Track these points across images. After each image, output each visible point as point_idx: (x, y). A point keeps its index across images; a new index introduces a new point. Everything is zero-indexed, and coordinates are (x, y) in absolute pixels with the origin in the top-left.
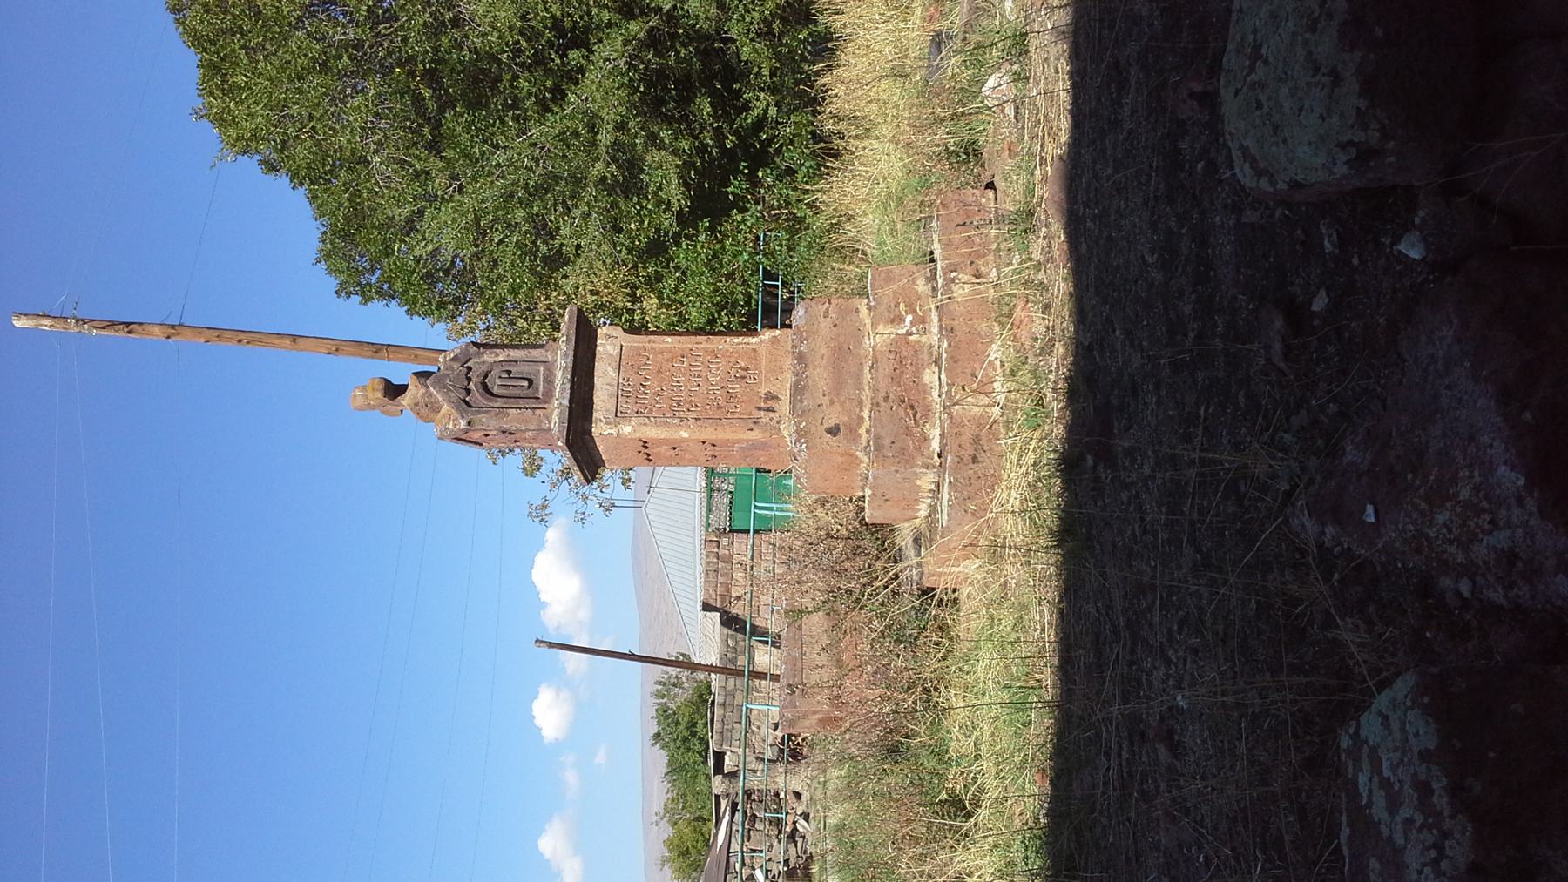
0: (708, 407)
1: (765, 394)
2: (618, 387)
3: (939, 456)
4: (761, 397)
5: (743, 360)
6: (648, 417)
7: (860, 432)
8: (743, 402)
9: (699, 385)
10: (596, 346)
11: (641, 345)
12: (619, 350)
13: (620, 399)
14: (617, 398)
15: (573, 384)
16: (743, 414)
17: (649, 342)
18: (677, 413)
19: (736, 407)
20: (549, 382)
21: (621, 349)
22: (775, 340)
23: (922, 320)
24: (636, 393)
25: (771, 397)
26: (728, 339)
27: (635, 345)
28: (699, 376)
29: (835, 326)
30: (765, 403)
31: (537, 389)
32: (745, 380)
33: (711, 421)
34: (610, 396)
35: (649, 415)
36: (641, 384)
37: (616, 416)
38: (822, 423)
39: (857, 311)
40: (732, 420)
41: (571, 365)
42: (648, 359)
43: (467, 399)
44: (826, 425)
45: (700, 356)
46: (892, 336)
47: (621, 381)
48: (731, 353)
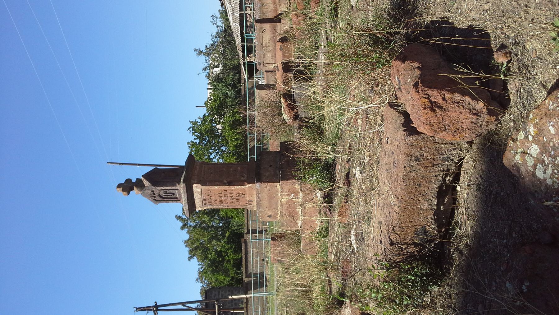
15: (188, 203)
20: (180, 194)
23: (297, 195)
25: (250, 201)
26: (235, 187)
29: (269, 190)
31: (176, 195)
34: (200, 201)
39: (276, 186)
41: (187, 199)
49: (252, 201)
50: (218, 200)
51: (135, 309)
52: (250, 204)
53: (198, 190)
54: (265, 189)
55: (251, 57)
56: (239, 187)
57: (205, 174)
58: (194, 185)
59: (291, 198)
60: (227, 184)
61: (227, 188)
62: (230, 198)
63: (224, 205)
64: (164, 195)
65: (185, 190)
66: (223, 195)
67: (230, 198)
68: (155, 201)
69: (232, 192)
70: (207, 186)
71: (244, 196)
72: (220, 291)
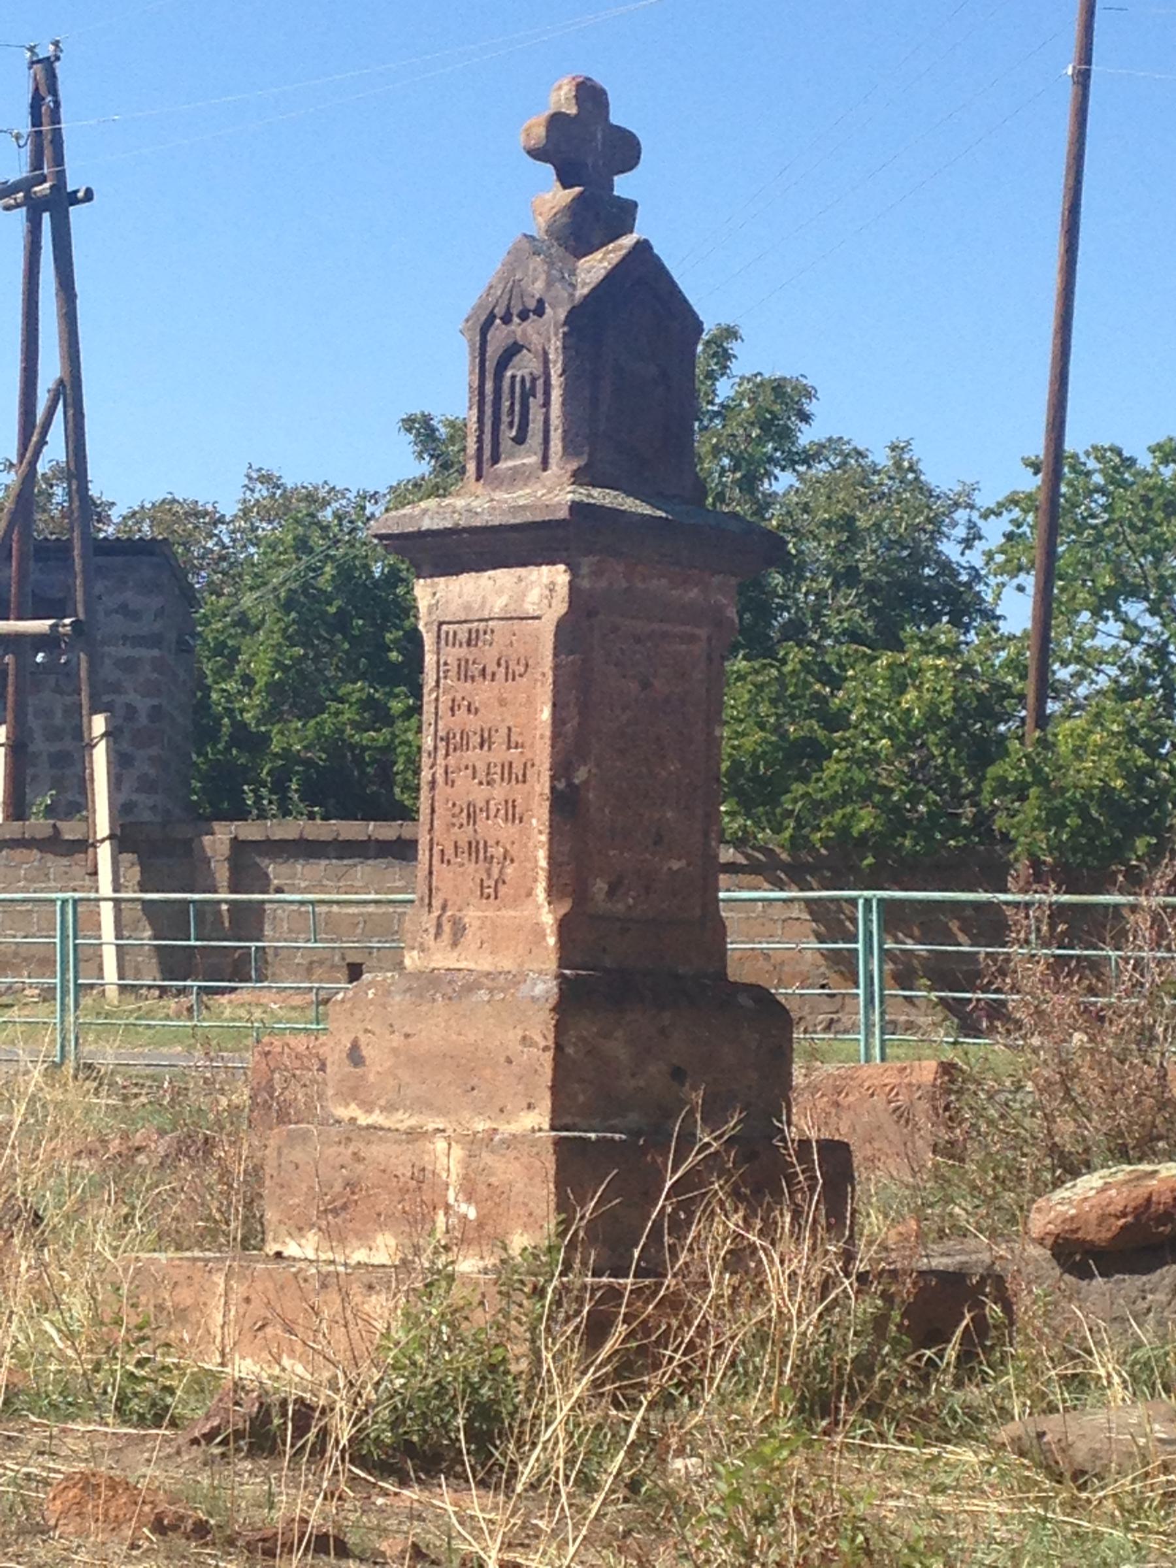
3: (279, 1255)
7: (353, 1106)
10: (539, 565)
12: (531, 613)
14: (465, 622)
20: (517, 477)
22: (538, 933)
25: (460, 930)
26: (544, 838)
31: (511, 456)
34: (467, 607)
37: (441, 624)
38: (366, 1031)
39: (530, 1107)
41: (478, 522)
43: (498, 321)
44: (363, 1039)
46: (444, 1175)
49: (455, 944)
50: (473, 723)
51: (48, 51)
52: (439, 926)
53: (534, 595)
54: (520, 1033)
56: (543, 863)
57: (638, 640)
58: (559, 575)
59: (451, 1201)
60: (561, 785)
61: (541, 784)
62: (481, 804)
63: (440, 761)
64: (513, 377)
65: (528, 517)
66: (499, 754)
67: (481, 804)
68: (483, 318)
69: (513, 813)
70: (555, 655)
71: (491, 891)
72: (156, 652)
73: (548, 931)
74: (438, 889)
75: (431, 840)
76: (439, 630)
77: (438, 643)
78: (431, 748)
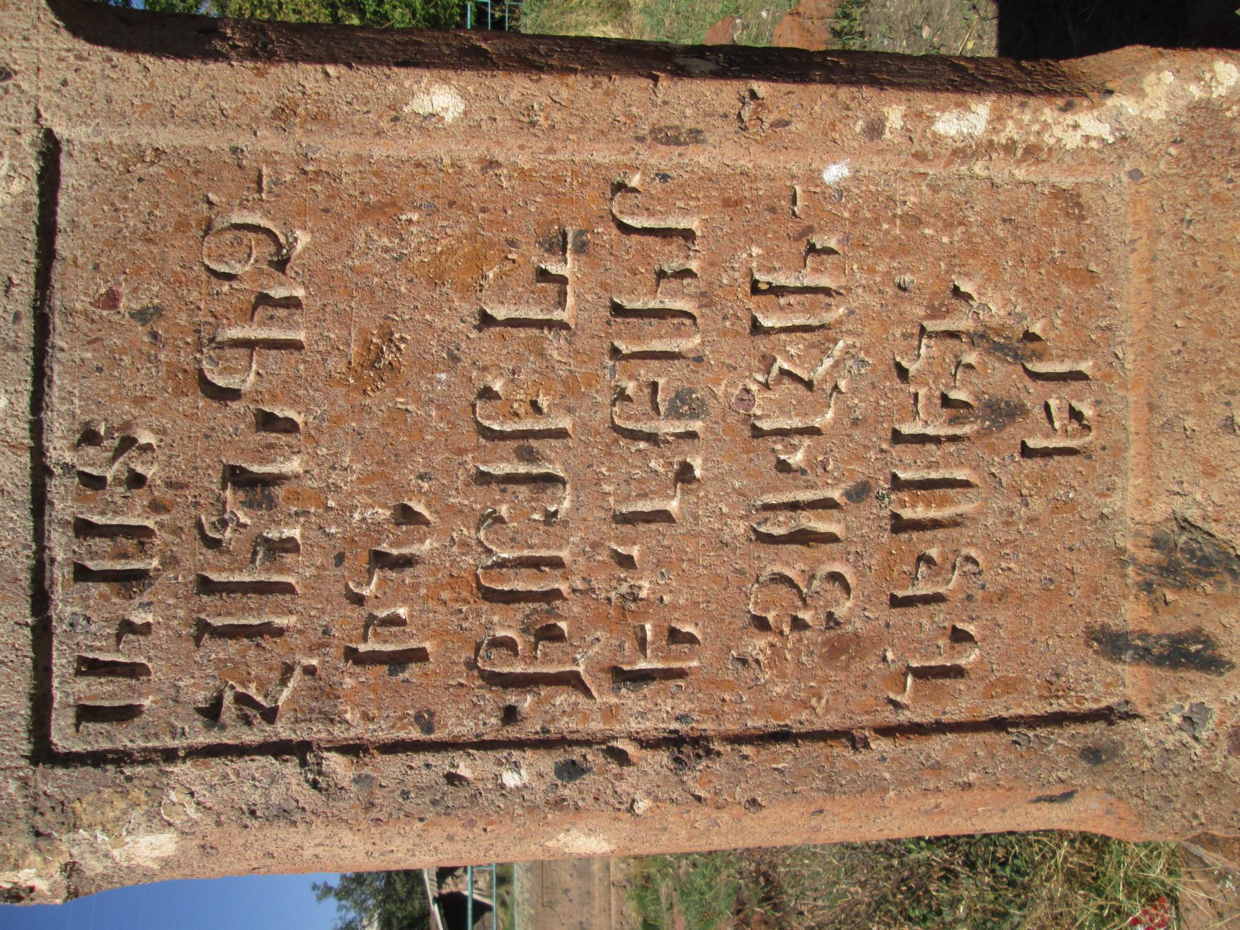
0: (758, 645)
1: (1157, 543)
2: (39, 503)
4: (1119, 557)
5: (994, 276)
6: (299, 750)
8: (1003, 595)
9: (685, 474)
11: (216, 141)
13: (63, 606)
14: (40, 600)
16: (1009, 686)
17: (283, 114)
18: (526, 703)
19: (959, 637)
21: (49, 180)
24: (196, 558)
26: (895, 115)
27: (164, 138)
28: (685, 405)
30: (1158, 605)
32: (1014, 433)
33: (784, 756)
35: (318, 732)
36: (236, 477)
40: (937, 746)
42: (281, 264)
45: (688, 235)
47: (59, 450)
48: (913, 221)
55: (457, 877)
73: (1195, 91)
74: (1050, 689)
75: (886, 731)
76: (69, 760)
77: (121, 758)
78: (547, 762)
